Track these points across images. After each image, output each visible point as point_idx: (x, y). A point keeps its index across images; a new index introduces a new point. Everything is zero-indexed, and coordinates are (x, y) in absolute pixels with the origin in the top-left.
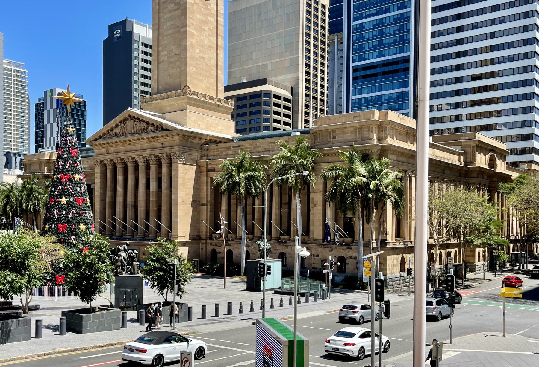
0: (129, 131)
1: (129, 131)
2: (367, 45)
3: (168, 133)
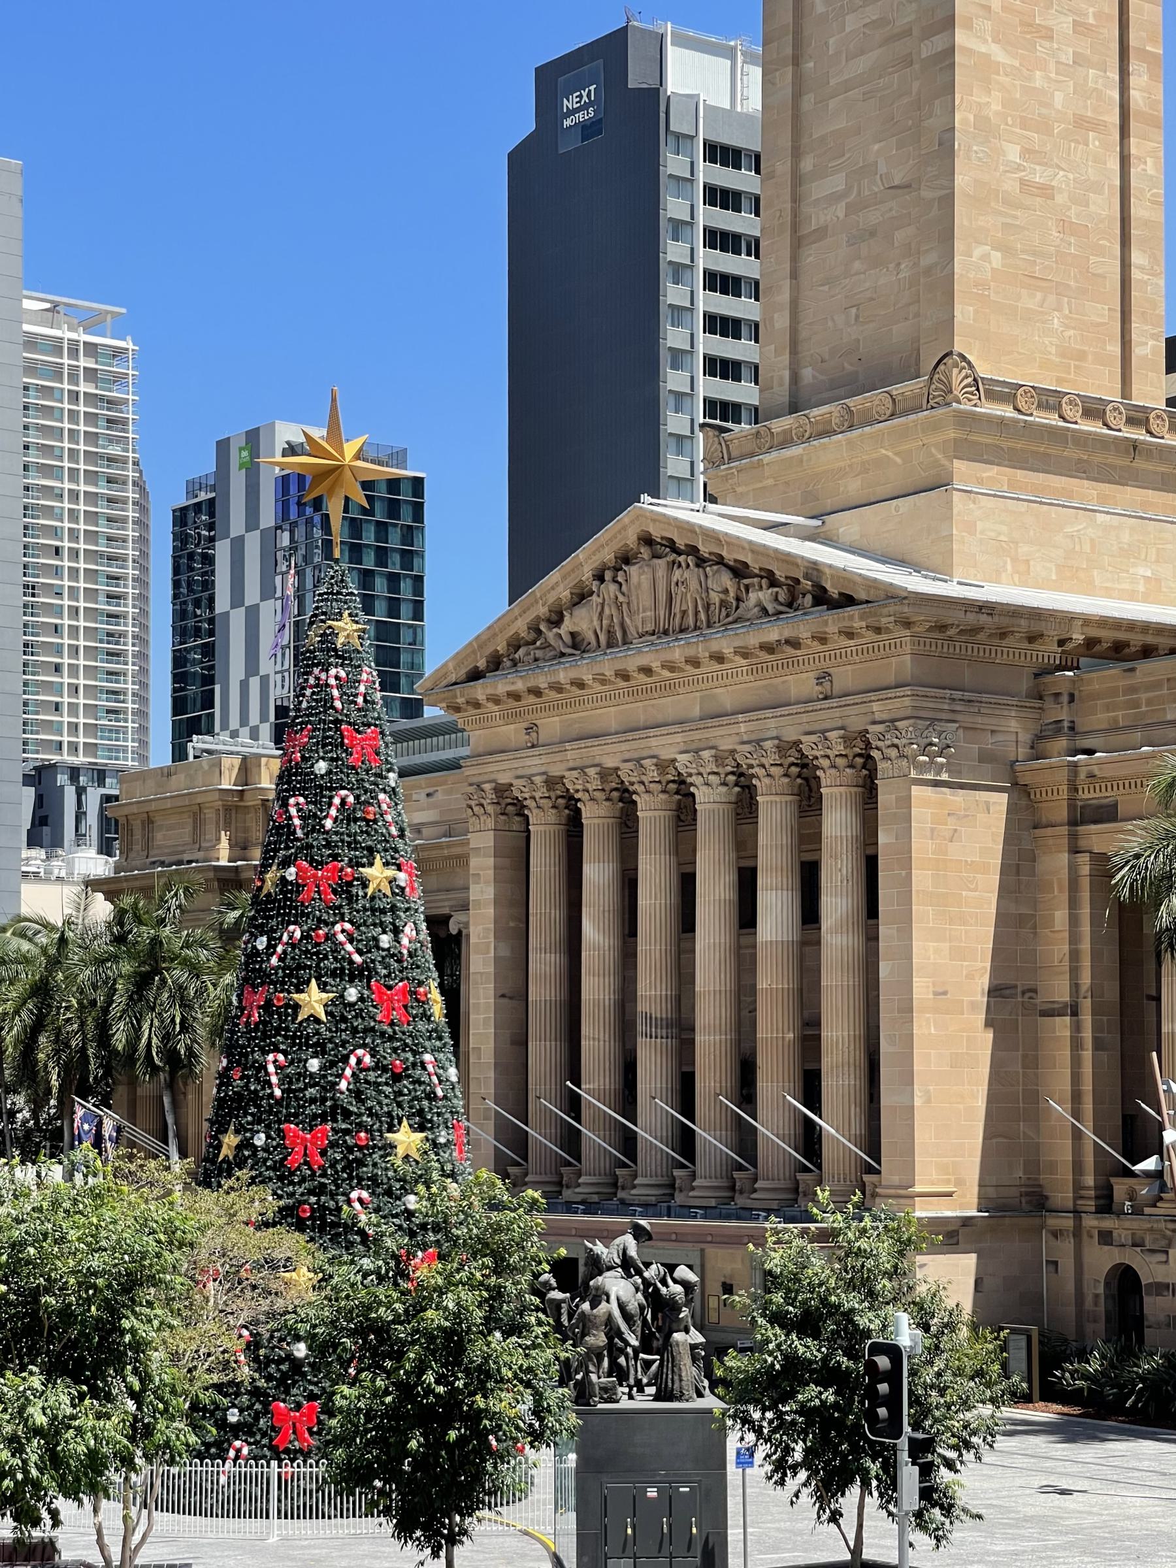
0: (642, 617)
3: (852, 617)
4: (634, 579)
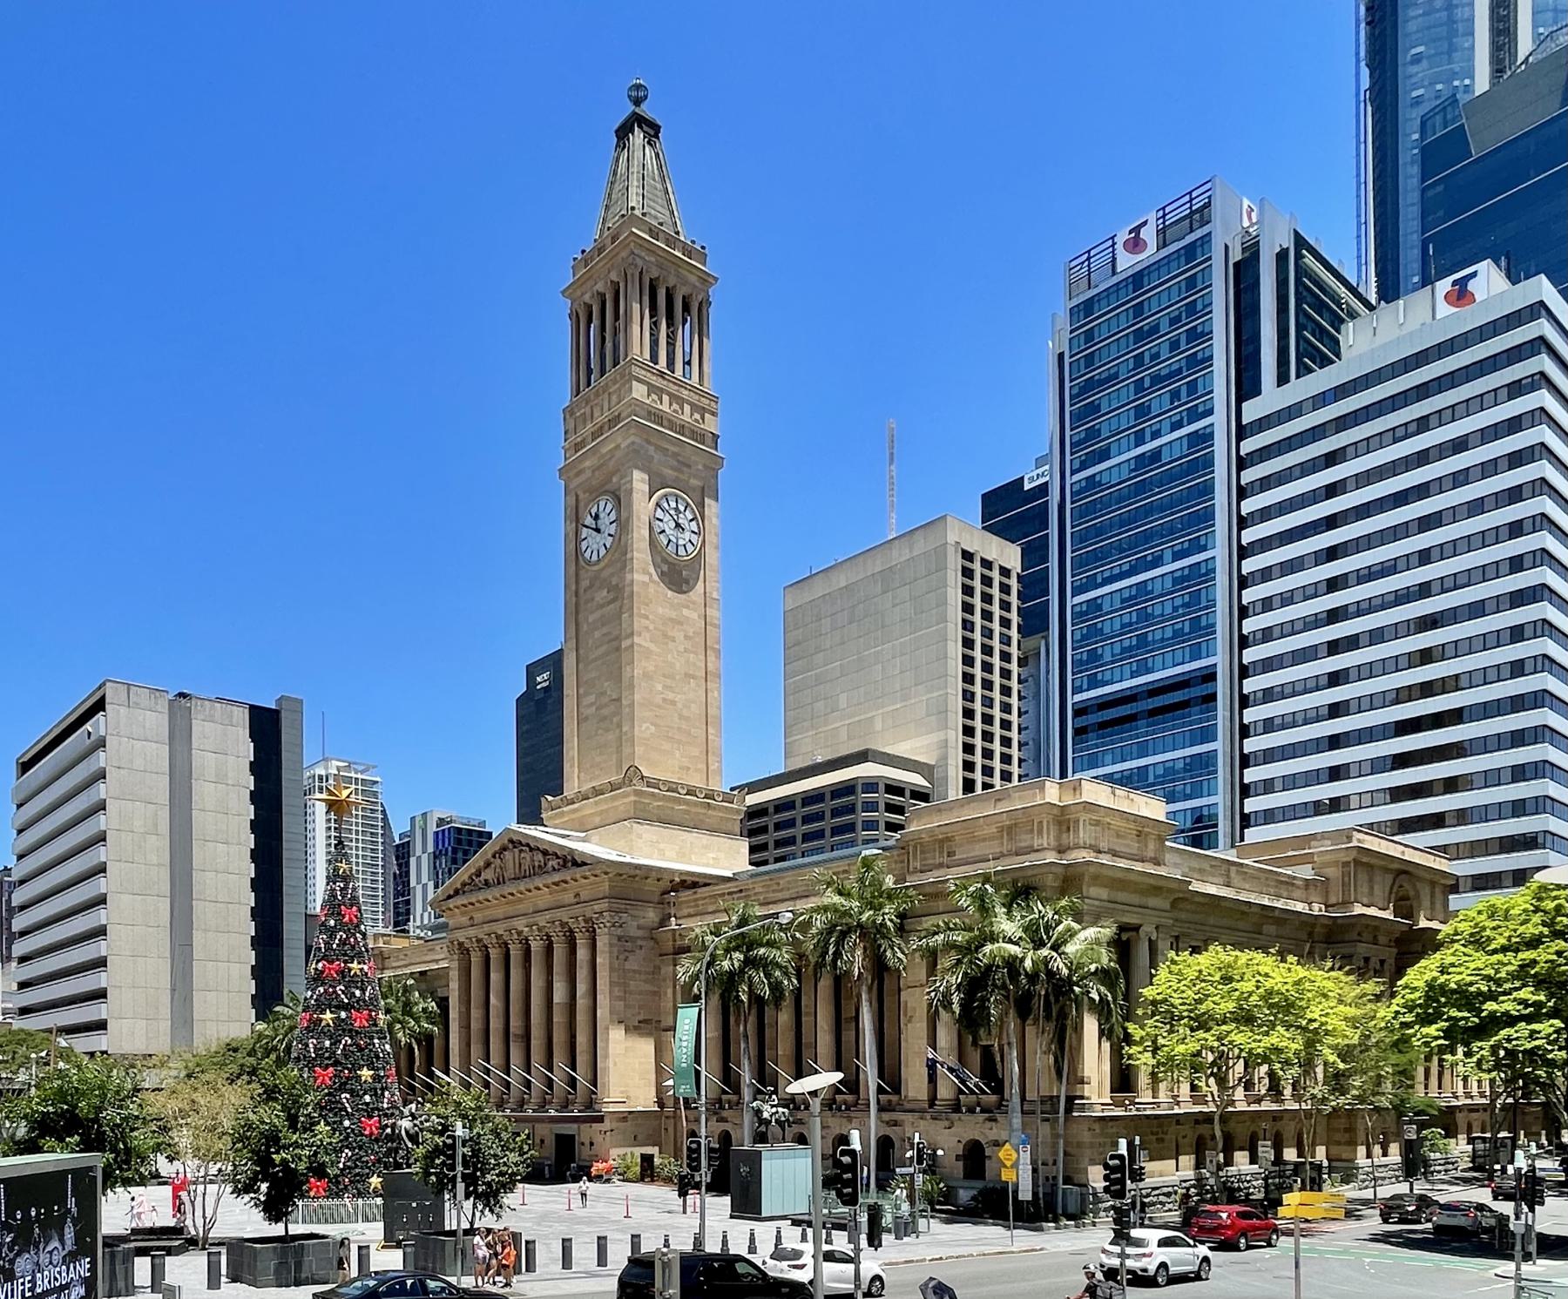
0: (509, 874)
1: (509, 874)
2: (1108, 649)
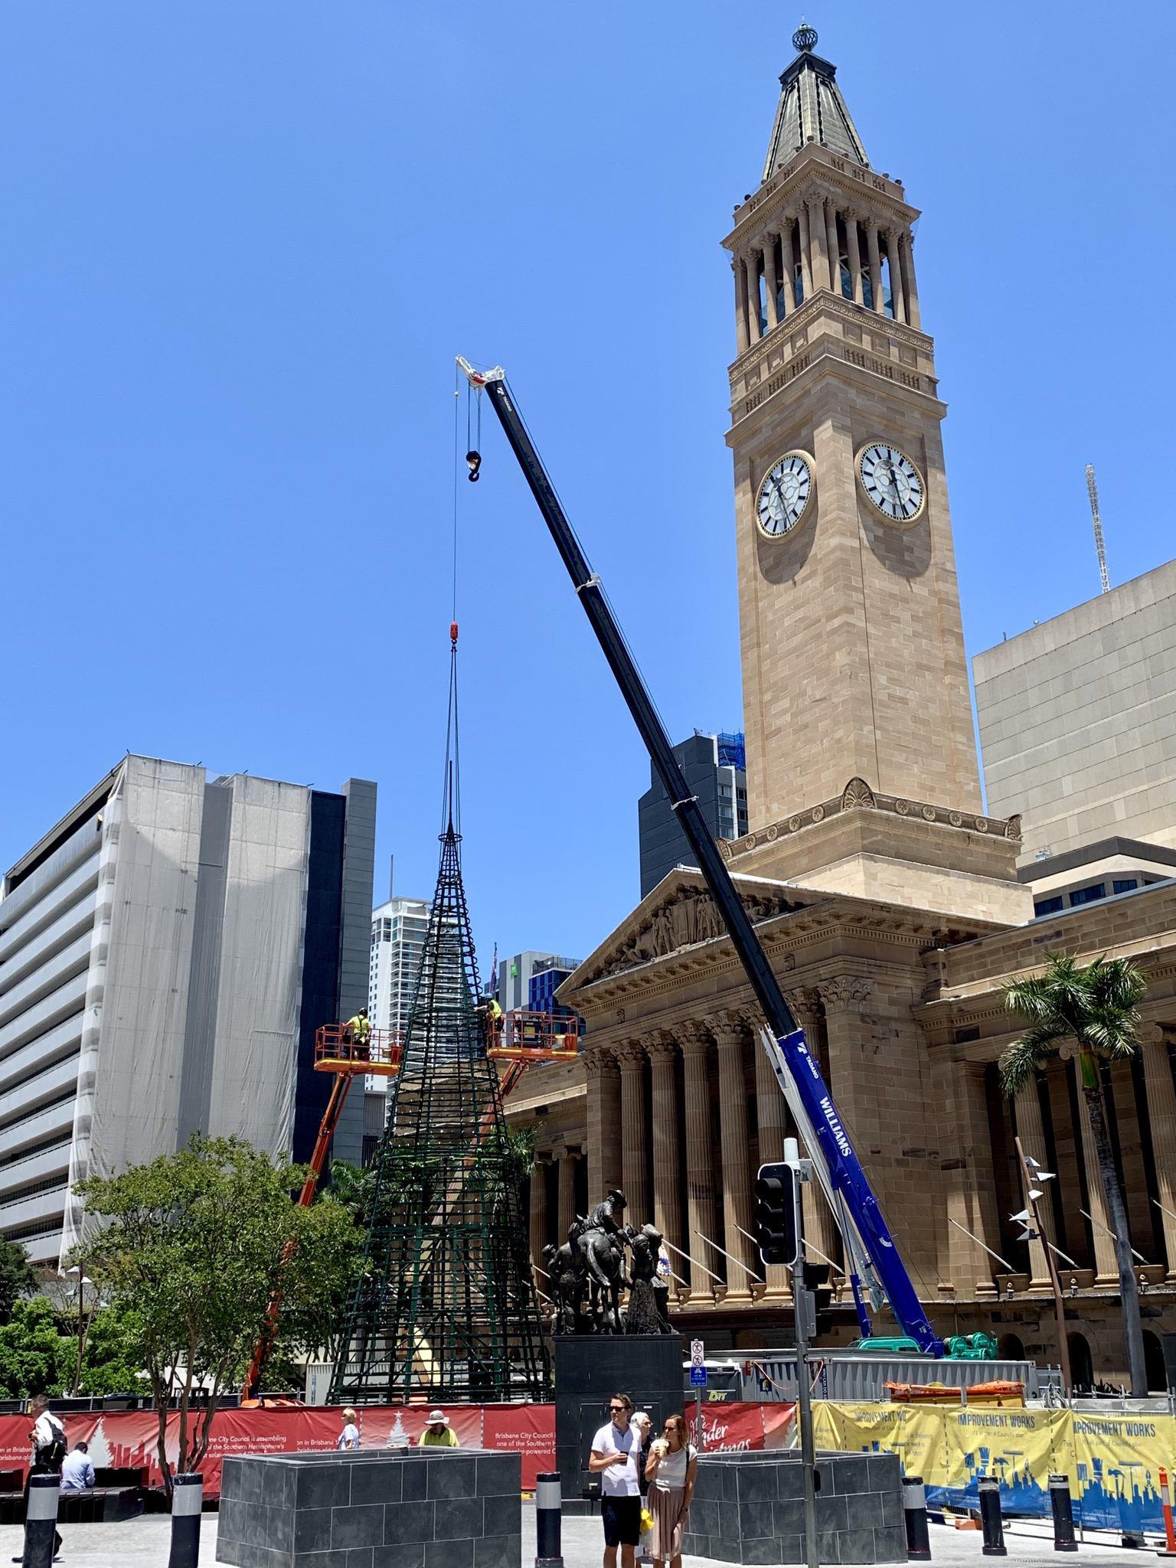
3: (804, 916)
4: (675, 913)
